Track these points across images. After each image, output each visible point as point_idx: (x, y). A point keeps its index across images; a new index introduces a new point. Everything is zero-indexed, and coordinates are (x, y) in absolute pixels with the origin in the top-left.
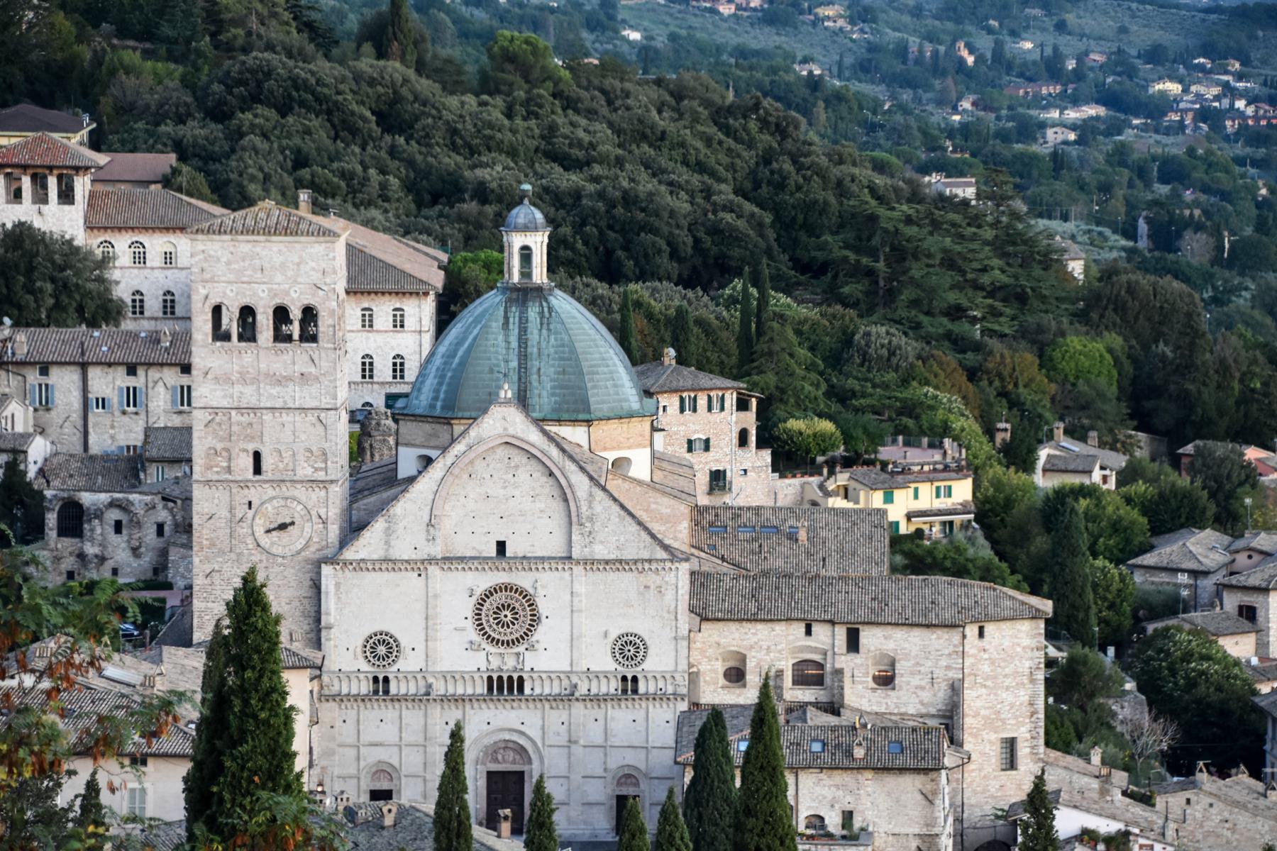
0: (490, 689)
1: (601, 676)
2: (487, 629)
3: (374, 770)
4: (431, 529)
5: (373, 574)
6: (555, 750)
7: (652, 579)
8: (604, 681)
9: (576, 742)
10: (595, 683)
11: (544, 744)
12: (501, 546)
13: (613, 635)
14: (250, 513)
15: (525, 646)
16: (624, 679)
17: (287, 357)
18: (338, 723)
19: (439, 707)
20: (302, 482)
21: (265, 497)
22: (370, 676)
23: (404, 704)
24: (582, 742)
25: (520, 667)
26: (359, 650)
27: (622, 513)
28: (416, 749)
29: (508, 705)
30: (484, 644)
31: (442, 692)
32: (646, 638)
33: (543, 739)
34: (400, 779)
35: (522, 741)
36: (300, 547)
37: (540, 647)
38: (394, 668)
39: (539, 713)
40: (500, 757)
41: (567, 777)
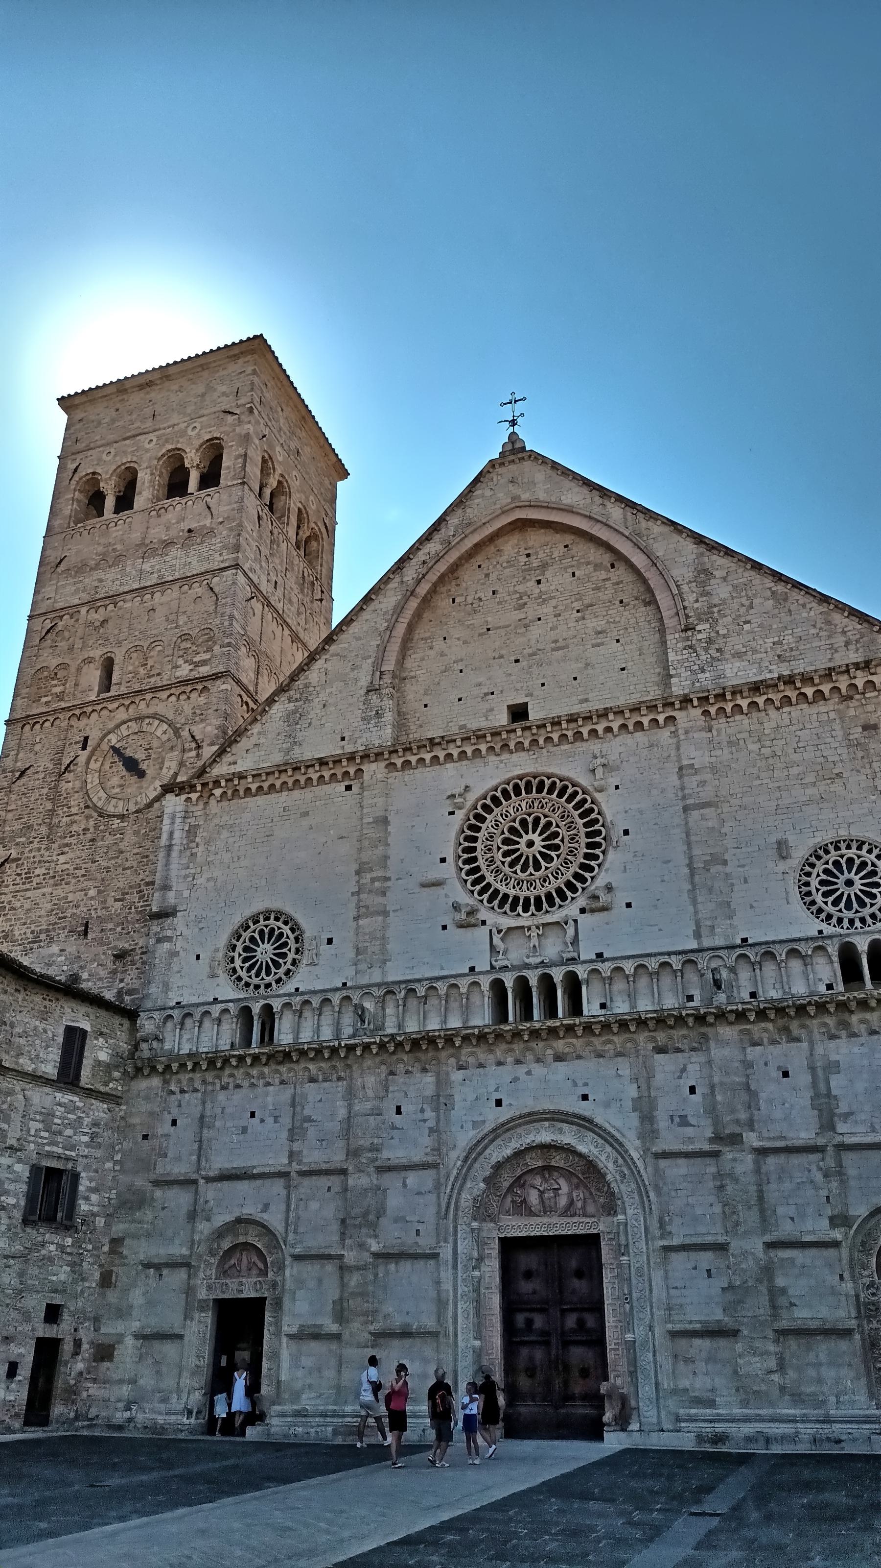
0: (501, 1014)
1: (781, 952)
2: (490, 878)
3: (226, 1244)
4: (374, 698)
5: (260, 800)
6: (678, 1169)
9: (735, 1140)
11: (646, 1150)
12: (519, 713)
13: (800, 853)
14: (84, 755)
15: (582, 902)
17: (171, 516)
20: (168, 687)
21: (111, 725)
24: (752, 1139)
26: (220, 955)
27: (780, 588)
28: (323, 1182)
30: (484, 914)
34: (281, 1267)
36: (152, 795)
37: (620, 899)
38: (289, 987)
40: (533, 1198)
41: (721, 1248)
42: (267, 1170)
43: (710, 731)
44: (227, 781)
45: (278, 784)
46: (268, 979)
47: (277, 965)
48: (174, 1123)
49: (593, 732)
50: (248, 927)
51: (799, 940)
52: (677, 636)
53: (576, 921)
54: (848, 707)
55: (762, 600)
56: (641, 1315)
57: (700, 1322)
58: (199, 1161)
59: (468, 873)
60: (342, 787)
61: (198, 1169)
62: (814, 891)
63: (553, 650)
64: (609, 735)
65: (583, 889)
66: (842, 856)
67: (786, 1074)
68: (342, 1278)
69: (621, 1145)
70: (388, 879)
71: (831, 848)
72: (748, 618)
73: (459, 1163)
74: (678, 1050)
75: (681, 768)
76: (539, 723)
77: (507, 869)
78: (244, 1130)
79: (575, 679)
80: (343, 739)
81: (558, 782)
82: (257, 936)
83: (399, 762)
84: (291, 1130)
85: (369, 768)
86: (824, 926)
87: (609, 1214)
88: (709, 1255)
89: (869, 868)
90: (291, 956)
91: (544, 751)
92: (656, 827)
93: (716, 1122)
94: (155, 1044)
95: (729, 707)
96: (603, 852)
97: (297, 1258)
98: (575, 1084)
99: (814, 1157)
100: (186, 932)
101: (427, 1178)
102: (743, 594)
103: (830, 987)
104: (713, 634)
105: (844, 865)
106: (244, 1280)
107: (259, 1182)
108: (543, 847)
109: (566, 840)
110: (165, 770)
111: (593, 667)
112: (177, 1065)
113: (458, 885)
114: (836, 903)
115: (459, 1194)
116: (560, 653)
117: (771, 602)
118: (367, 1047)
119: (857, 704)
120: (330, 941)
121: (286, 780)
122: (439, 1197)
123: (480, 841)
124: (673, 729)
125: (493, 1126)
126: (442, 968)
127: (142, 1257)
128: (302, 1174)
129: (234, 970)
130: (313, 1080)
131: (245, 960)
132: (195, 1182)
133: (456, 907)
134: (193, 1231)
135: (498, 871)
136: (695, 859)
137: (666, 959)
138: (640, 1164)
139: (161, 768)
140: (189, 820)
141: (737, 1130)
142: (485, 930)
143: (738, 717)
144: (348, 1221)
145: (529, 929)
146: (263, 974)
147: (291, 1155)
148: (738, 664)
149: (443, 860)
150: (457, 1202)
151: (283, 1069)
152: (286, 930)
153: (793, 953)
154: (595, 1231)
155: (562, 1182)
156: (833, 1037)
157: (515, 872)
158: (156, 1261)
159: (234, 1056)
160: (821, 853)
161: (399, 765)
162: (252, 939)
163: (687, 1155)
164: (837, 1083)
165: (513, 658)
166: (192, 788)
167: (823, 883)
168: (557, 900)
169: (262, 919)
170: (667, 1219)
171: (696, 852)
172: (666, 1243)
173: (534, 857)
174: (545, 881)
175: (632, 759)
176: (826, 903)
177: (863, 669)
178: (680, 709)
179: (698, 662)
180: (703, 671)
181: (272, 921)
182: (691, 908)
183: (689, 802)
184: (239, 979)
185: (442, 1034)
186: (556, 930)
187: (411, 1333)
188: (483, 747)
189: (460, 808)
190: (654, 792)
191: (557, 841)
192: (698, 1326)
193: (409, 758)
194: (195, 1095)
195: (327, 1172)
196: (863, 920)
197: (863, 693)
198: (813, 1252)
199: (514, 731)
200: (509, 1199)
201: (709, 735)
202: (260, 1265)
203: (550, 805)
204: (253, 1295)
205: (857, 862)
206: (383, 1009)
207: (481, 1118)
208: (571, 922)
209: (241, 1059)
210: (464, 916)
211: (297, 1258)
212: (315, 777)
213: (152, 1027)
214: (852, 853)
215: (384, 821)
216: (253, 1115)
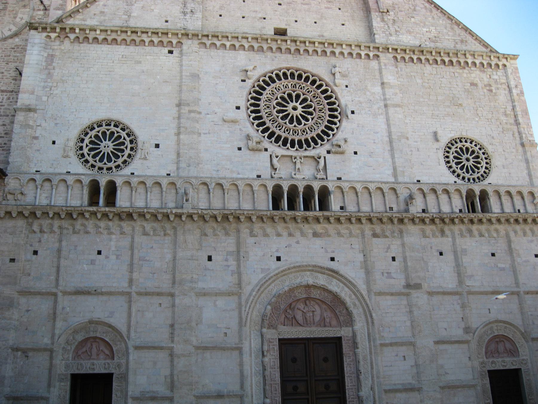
3: (80, 337)
5: (105, 48)
6: (386, 302)
7: (476, 75)
8: (444, 198)
9: (418, 286)
10: (431, 198)
11: (369, 291)
13: (445, 140)
16: (470, 195)
18: (25, 255)
19: (197, 232)
22: (86, 180)
23: (139, 223)
25: (321, 175)
26: (72, 143)
28: (156, 300)
29: (308, 229)
30: (266, 143)
31: (203, 205)
32: (485, 144)
33: (368, 282)
34: (127, 353)
35: (335, 286)
36: (8, 33)
37: (349, 149)
38: (127, 171)
39: (357, 244)
40: (299, 317)
42: (113, 290)
43: (397, 67)
44: (80, 30)
45: (119, 39)
46: (110, 165)
47: (117, 157)
48: (35, 253)
49: (333, 53)
50: (94, 128)
51: (448, 184)
52: (377, 14)
53: (325, 158)
54: (464, 73)
55: (420, 9)
56: (367, 382)
57: (401, 384)
58: (57, 280)
59: (254, 119)
60: (166, 50)
61: (57, 285)
62: (451, 161)
63: (302, 4)
64: (341, 57)
65: (328, 140)
66: (464, 146)
67: (441, 254)
68: (172, 361)
69: (354, 286)
70: (200, 113)
71: (458, 141)
72: (414, 15)
73: (254, 293)
74: (386, 237)
75: (383, 84)
76: (302, 39)
77: (280, 120)
78: (93, 262)
79: (315, 23)
80: (167, 21)
81: (311, 76)
82: (100, 134)
83: (208, 43)
84: (131, 265)
85: (187, 44)
86: (456, 179)
87: (347, 326)
88: (404, 348)
89: (476, 154)
90: (127, 152)
91: (302, 57)
92: (369, 112)
93: (407, 278)
94: (19, 196)
95: (407, 57)
96: (339, 121)
97: (137, 348)
98: (326, 252)
99: (457, 297)
100: (44, 124)
101: (232, 302)
102: (410, 3)
103: (461, 211)
104: (396, 18)
105: (465, 150)
106: (95, 362)
107: (105, 298)
108: (302, 112)
109: (317, 110)
110: (18, 20)
111: (325, 19)
112: (40, 212)
113: (249, 125)
114: (462, 169)
115: (252, 312)
116: (306, 7)
117: (424, 10)
118: (190, 216)
119: (468, 72)
120: (157, 146)
121: (126, 38)
122: (240, 313)
123: (262, 101)
124: (377, 62)
125: (277, 272)
126: (239, 174)
127: (11, 343)
128: (139, 294)
129: (83, 155)
130: (145, 234)
131: (91, 150)
132: (55, 295)
133: (248, 137)
134: (54, 327)
135: (274, 121)
136: (393, 134)
137: (380, 185)
138: (366, 297)
139: (15, 18)
140: (47, 51)
141: (419, 281)
142: (267, 154)
143: (411, 64)
144: (176, 326)
145: (295, 158)
146: (105, 160)
147: (131, 281)
148: (410, 37)
149: (238, 108)
150: (251, 317)
151: (124, 224)
152: (123, 134)
153: (446, 191)
154: (339, 336)
155: (317, 307)
156: (465, 237)
157: (286, 123)
158: (23, 346)
159: (88, 211)
160: (453, 142)
161: (208, 45)
162: (97, 136)
163: (392, 294)
164: (465, 260)
165: (277, 2)
166: (53, 29)
167: (455, 157)
168: (312, 144)
169: (104, 125)
170: (381, 328)
171: (393, 129)
172: (382, 342)
173: (297, 117)
174: (304, 131)
175: (355, 73)
176: (457, 168)
177: (471, 55)
178: (382, 52)
179: (389, 31)
180: (391, 35)
181: (112, 127)
182: (390, 160)
183: (388, 102)
184: (87, 161)
185: (245, 213)
186: (311, 161)
187: (223, 396)
188: (265, 47)
189: (249, 79)
190: (368, 93)
191: (311, 110)
192: (400, 387)
193: (215, 42)
194: (52, 235)
195: (159, 294)
196: (474, 179)
197: (470, 68)
198: (456, 346)
199: (286, 41)
200: (284, 316)
201: (396, 70)
202: (107, 352)
203: (306, 88)
204: (103, 371)
205: (471, 150)
206: (198, 193)
207: (267, 267)
208: (322, 158)
209: (94, 214)
210: (254, 144)
211: (137, 348)
212: (147, 40)
213: (17, 185)
214: (468, 145)
215: (195, 77)
216: (99, 253)
